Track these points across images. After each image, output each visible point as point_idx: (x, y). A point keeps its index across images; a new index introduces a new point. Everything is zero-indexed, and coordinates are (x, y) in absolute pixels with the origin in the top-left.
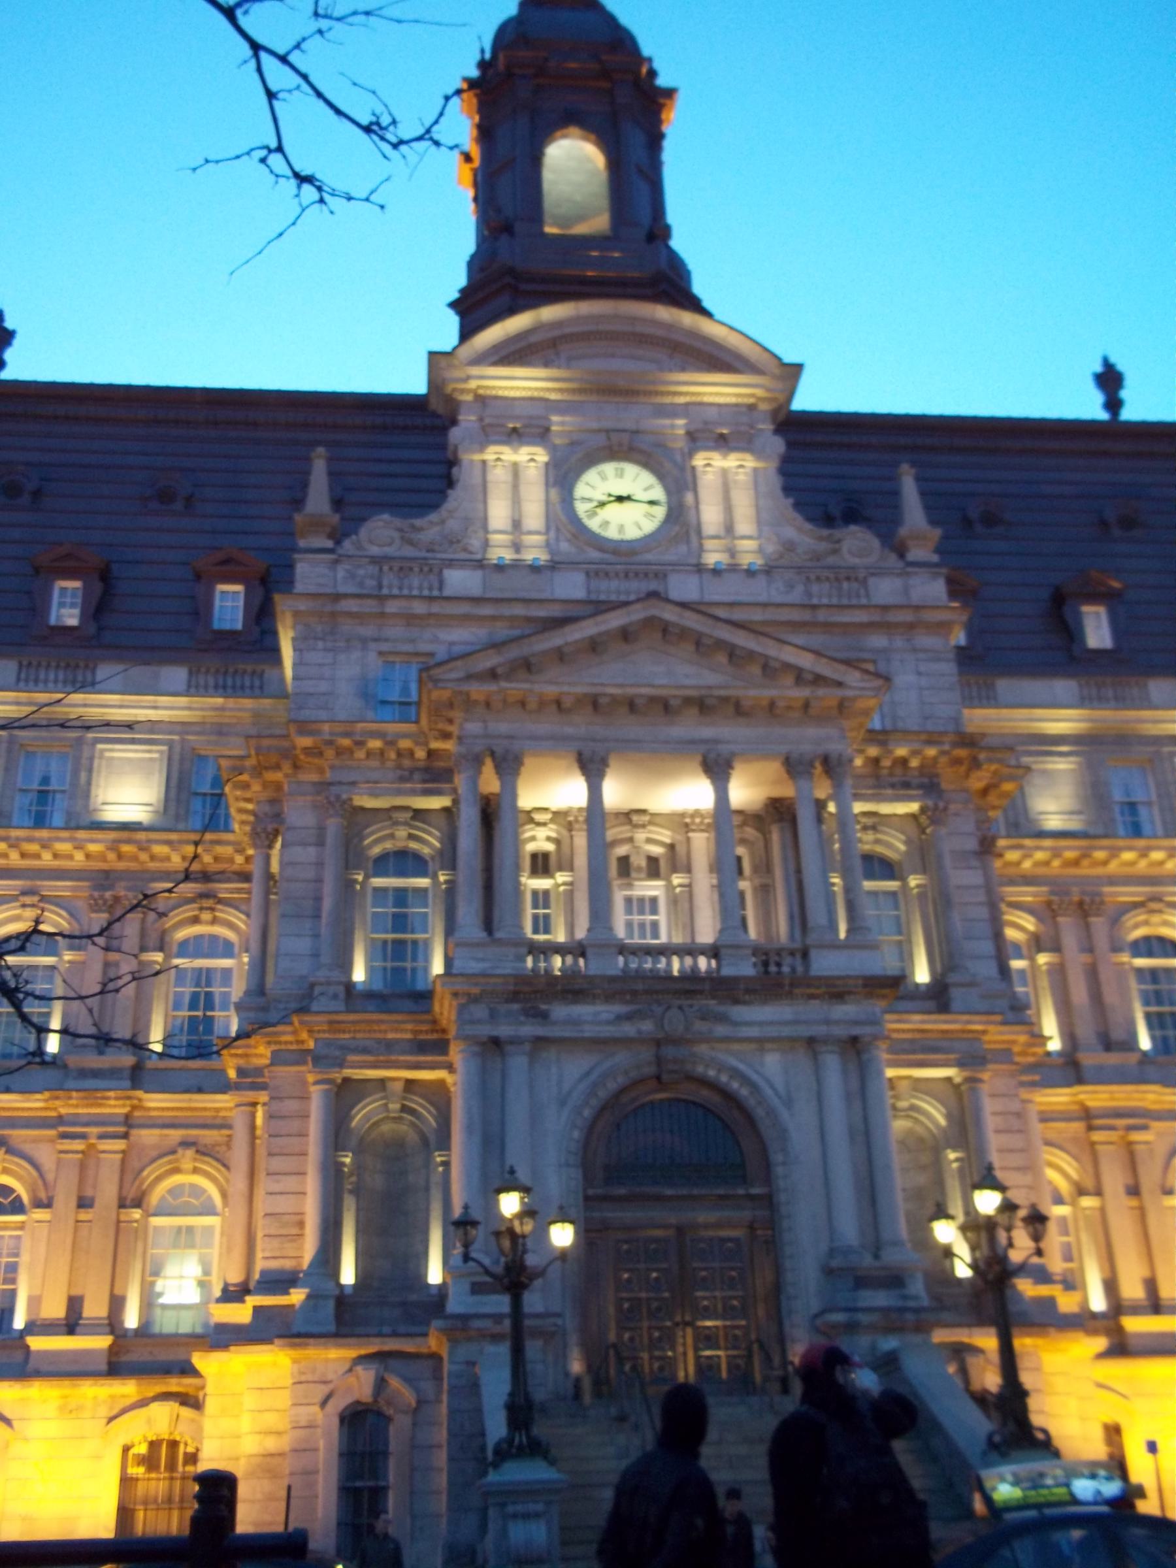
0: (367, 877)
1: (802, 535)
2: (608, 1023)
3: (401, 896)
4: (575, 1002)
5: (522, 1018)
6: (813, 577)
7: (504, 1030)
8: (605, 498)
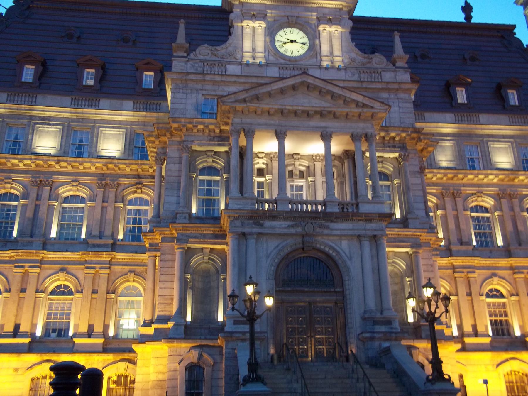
0: (197, 176)
1: (358, 56)
2: (285, 228)
3: (209, 183)
4: (273, 220)
5: (254, 226)
6: (361, 71)
7: (247, 230)
8: (287, 41)
